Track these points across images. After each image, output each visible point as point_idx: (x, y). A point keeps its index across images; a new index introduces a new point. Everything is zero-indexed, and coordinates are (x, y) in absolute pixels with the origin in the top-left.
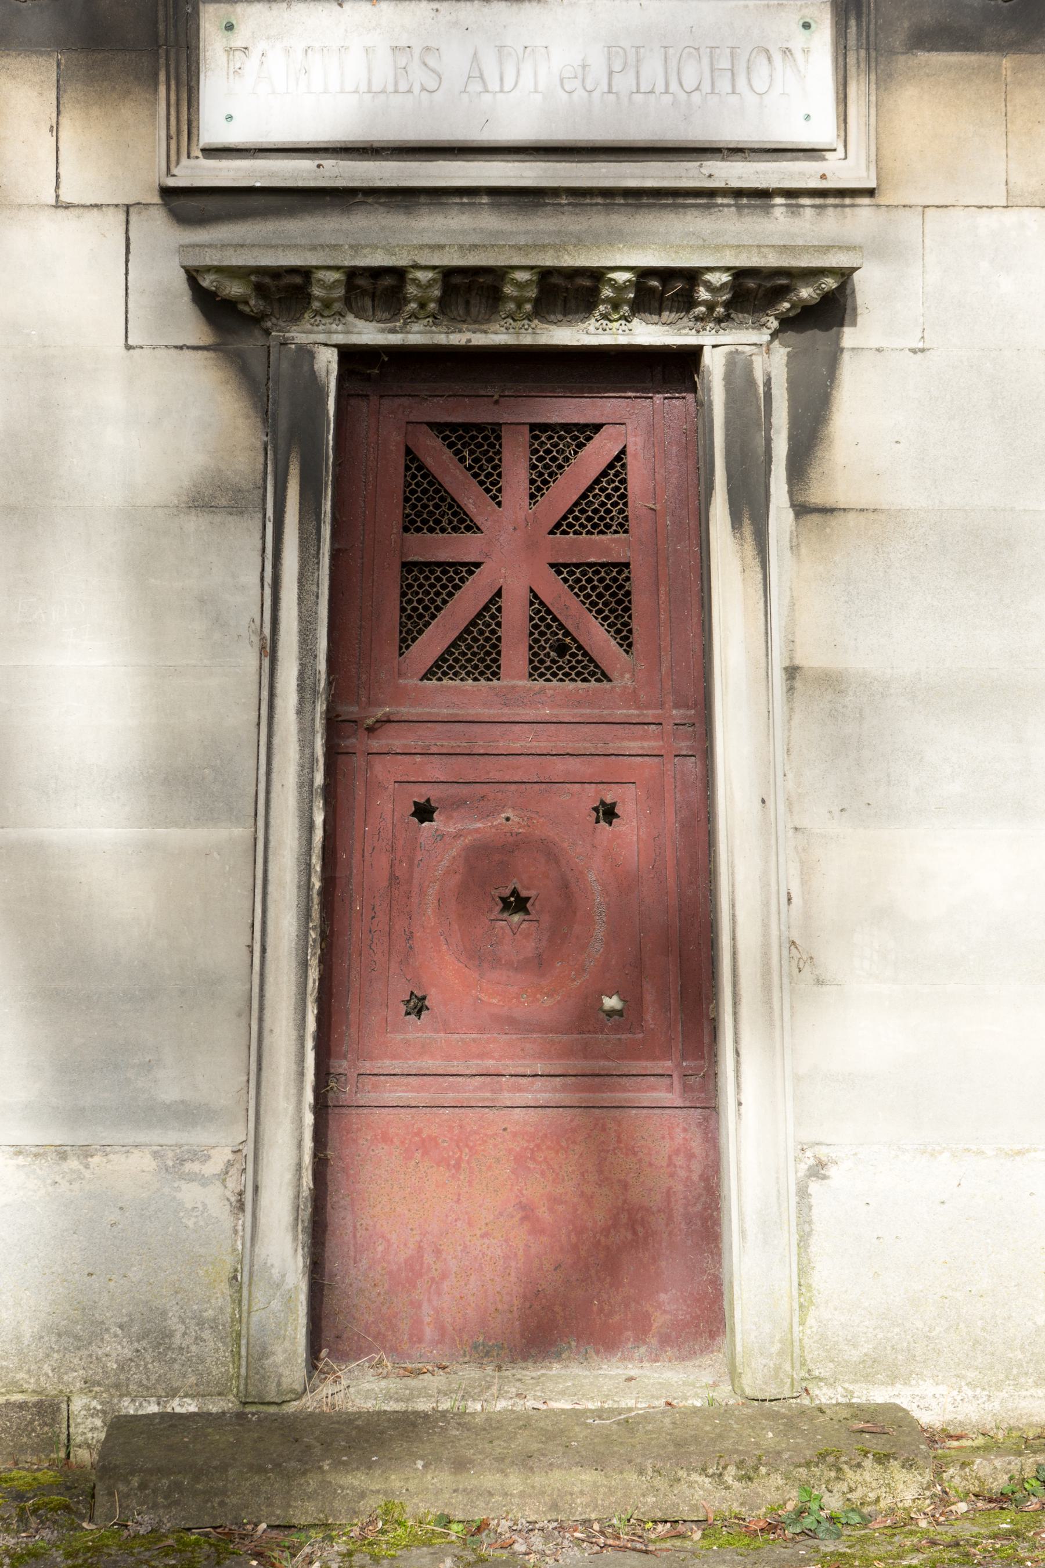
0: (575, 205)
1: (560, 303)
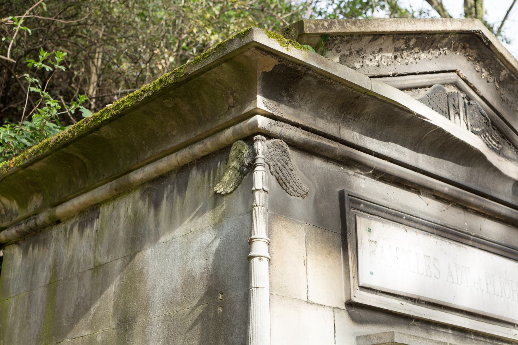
0: (476, 340)
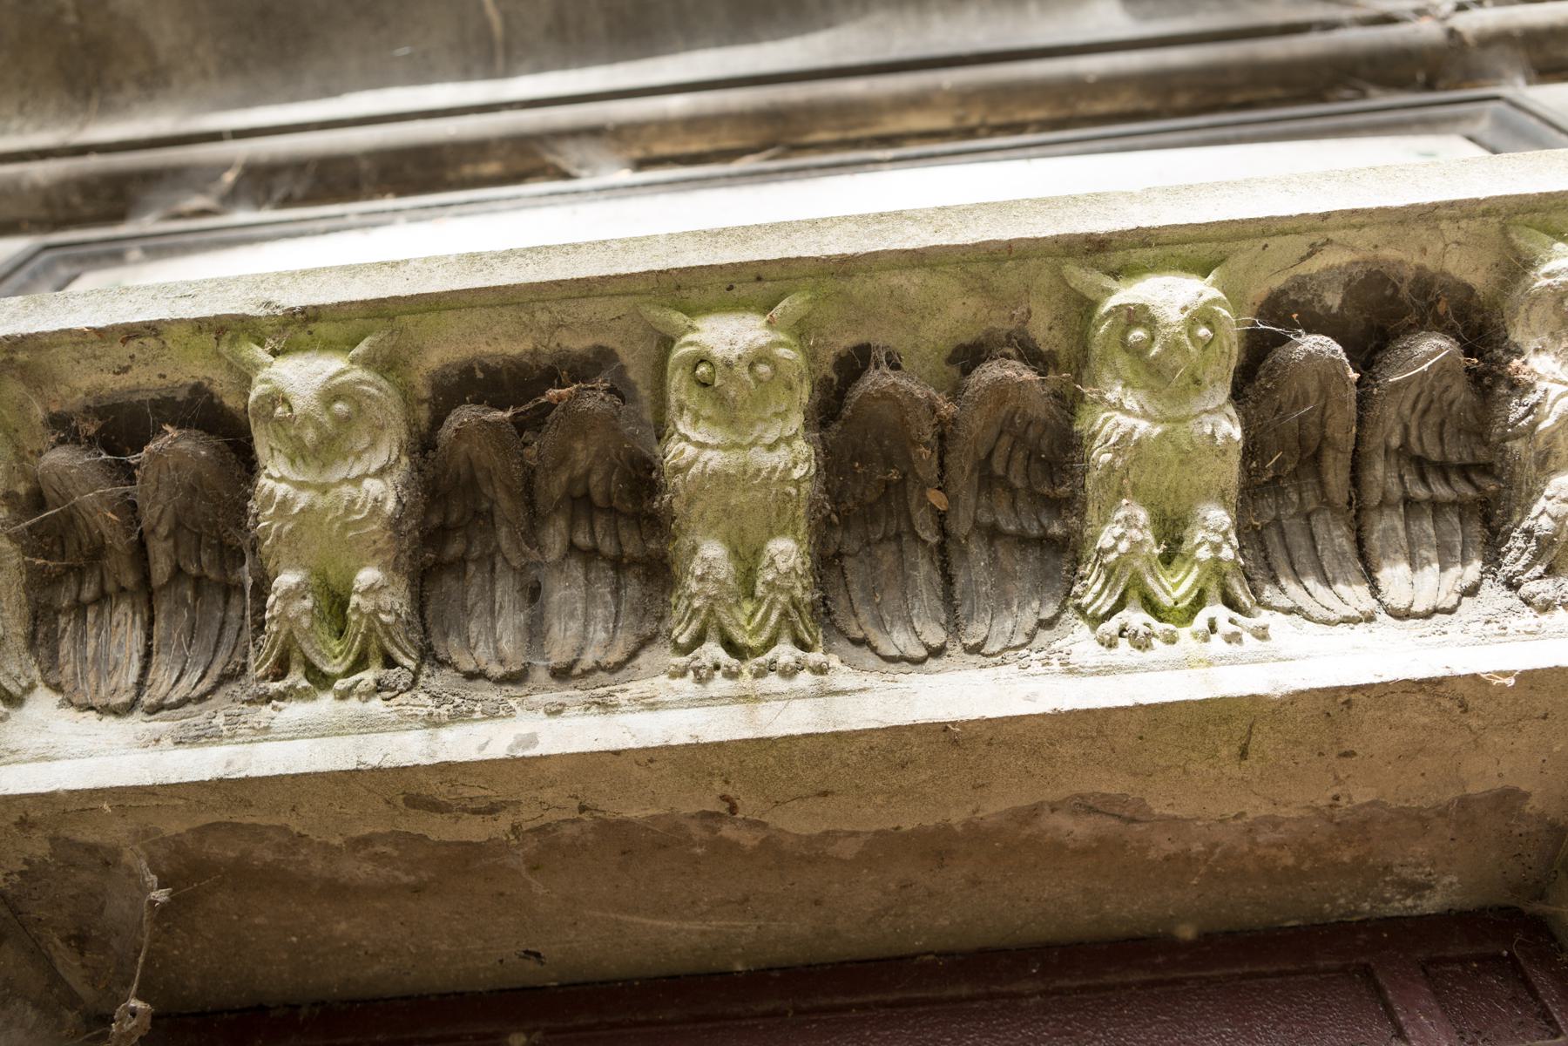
1: (923, 571)
